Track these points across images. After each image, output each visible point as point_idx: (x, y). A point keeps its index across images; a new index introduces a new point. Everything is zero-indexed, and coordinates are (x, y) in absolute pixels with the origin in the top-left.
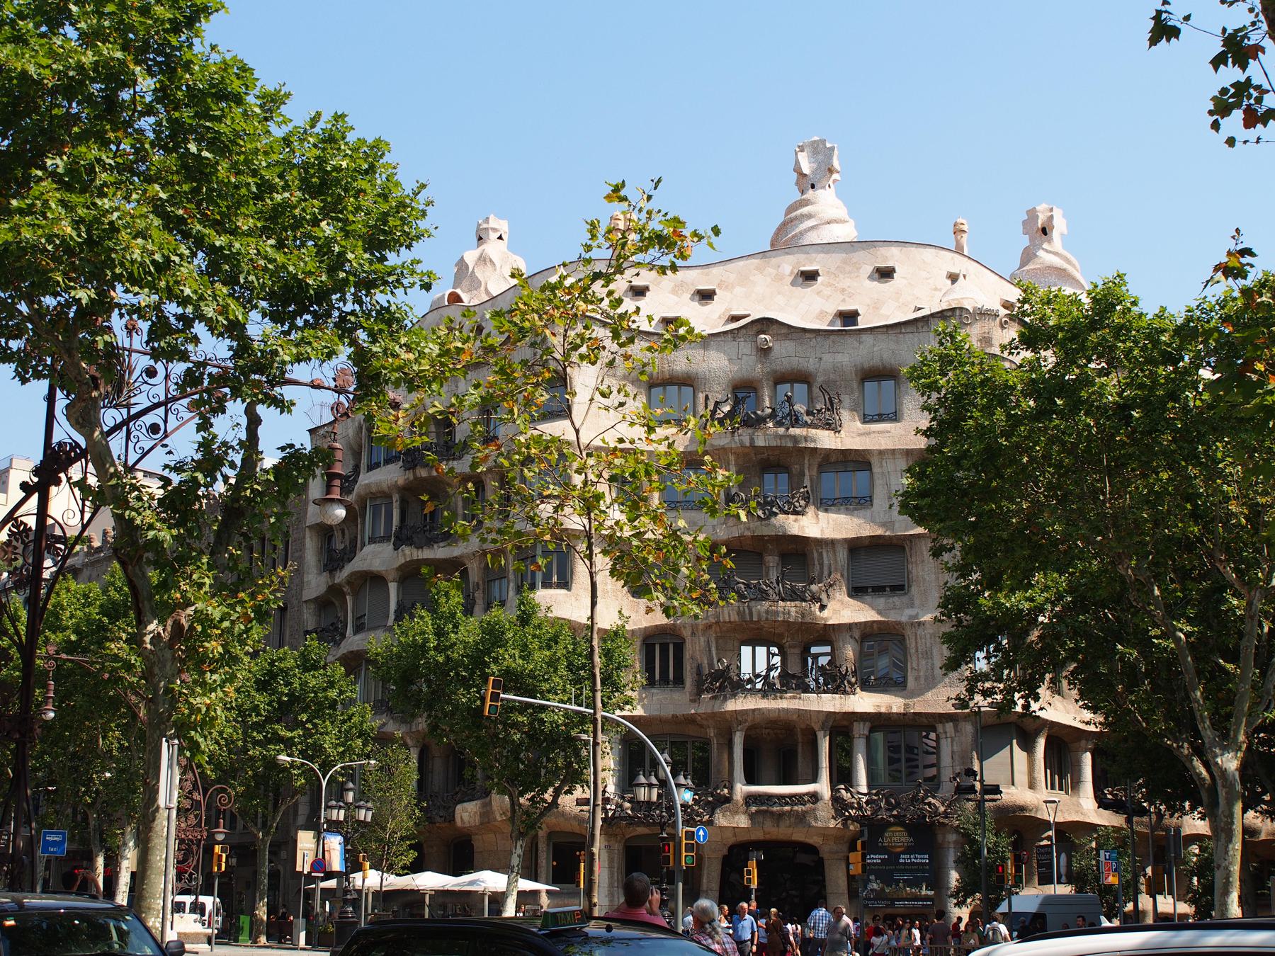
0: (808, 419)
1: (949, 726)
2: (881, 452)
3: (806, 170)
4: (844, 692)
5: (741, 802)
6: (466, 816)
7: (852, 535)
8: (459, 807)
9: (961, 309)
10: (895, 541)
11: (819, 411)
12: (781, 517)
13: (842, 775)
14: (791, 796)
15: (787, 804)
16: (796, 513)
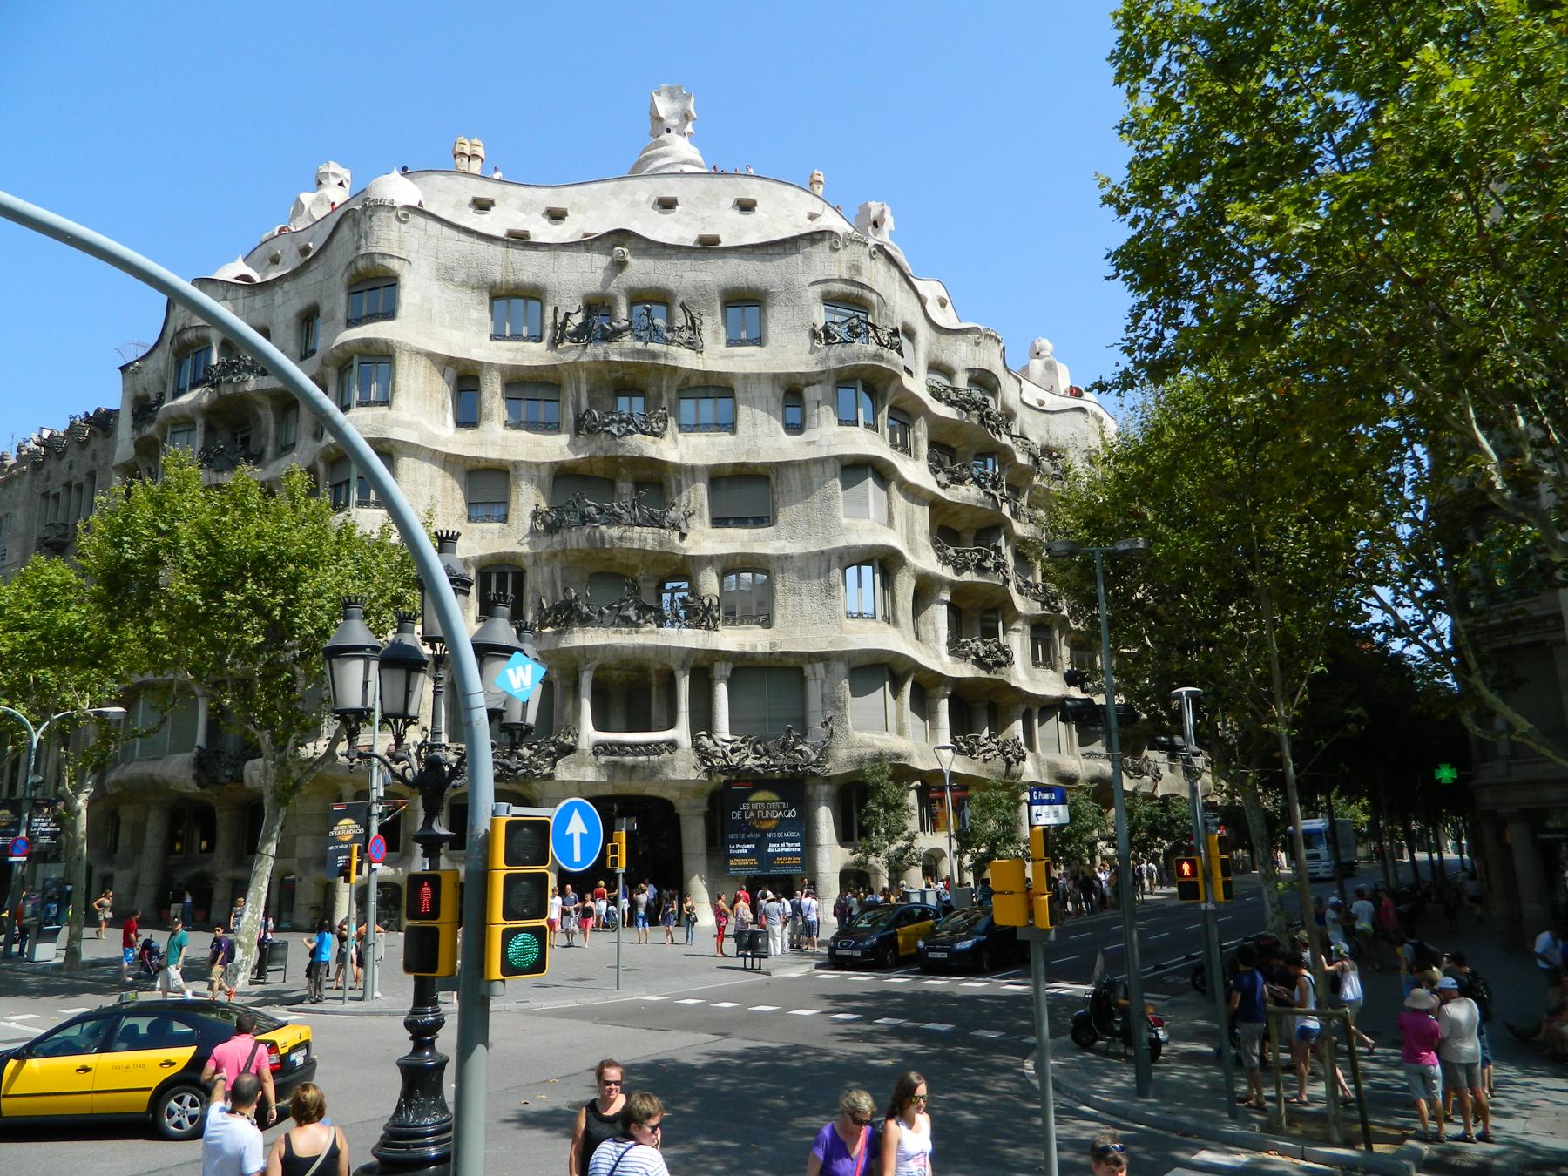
0: (669, 336)
1: (820, 667)
2: (746, 376)
3: (662, 114)
4: (708, 628)
5: (589, 750)
6: (256, 775)
7: (713, 461)
8: (248, 764)
9: (831, 232)
10: (760, 470)
11: (680, 329)
12: (638, 436)
13: (703, 720)
14: (649, 744)
15: (640, 754)
16: (655, 435)
